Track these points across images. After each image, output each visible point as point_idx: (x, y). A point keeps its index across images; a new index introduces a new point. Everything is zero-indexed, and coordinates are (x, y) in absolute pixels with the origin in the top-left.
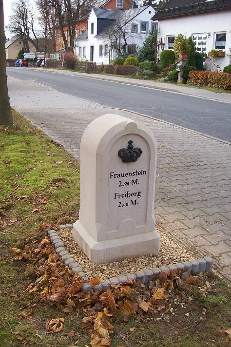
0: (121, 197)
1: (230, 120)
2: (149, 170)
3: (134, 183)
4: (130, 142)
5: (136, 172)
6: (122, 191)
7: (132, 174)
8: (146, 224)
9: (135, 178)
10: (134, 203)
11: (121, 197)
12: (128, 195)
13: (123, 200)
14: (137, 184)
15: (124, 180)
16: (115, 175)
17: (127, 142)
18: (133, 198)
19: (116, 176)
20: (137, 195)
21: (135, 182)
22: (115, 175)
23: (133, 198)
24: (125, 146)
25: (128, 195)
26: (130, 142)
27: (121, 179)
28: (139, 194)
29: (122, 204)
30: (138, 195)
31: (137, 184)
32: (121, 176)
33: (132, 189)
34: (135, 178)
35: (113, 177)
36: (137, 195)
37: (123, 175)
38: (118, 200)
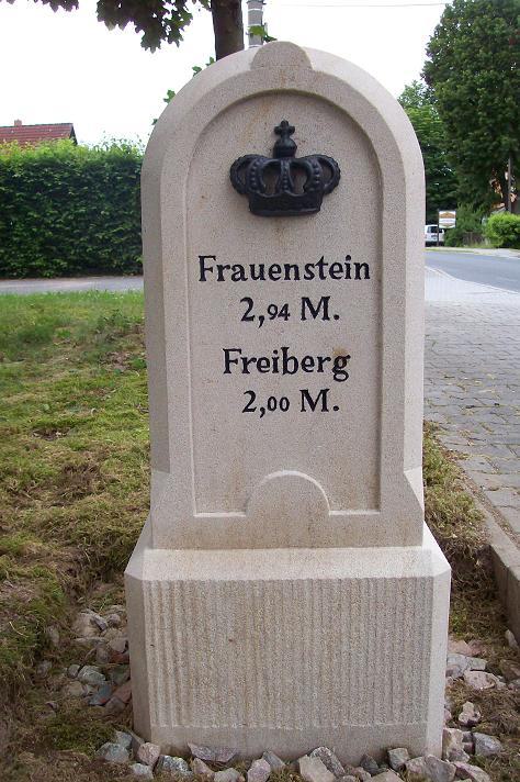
0: (252, 367)
1: (517, 420)
2: (379, 258)
3: (315, 314)
4: (284, 131)
5: (321, 264)
6: (259, 341)
7: (302, 272)
8: (377, 507)
9: (315, 289)
10: (315, 401)
11: (252, 367)
12: (284, 362)
13: (266, 384)
14: (326, 317)
15: (268, 293)
16: (221, 268)
17: (270, 130)
18: (315, 382)
19: (227, 274)
20: (328, 366)
21: (319, 309)
22: (221, 268)
23: (315, 382)
24: (260, 145)
25: (284, 362)
26: (284, 131)
27: (248, 287)
28: (340, 364)
29: (261, 402)
30: (336, 370)
31: (326, 317)
32: (247, 274)
33: (304, 337)
34: (315, 289)
35: (212, 276)
36: (328, 366)
37: (259, 273)
38: (239, 381)
